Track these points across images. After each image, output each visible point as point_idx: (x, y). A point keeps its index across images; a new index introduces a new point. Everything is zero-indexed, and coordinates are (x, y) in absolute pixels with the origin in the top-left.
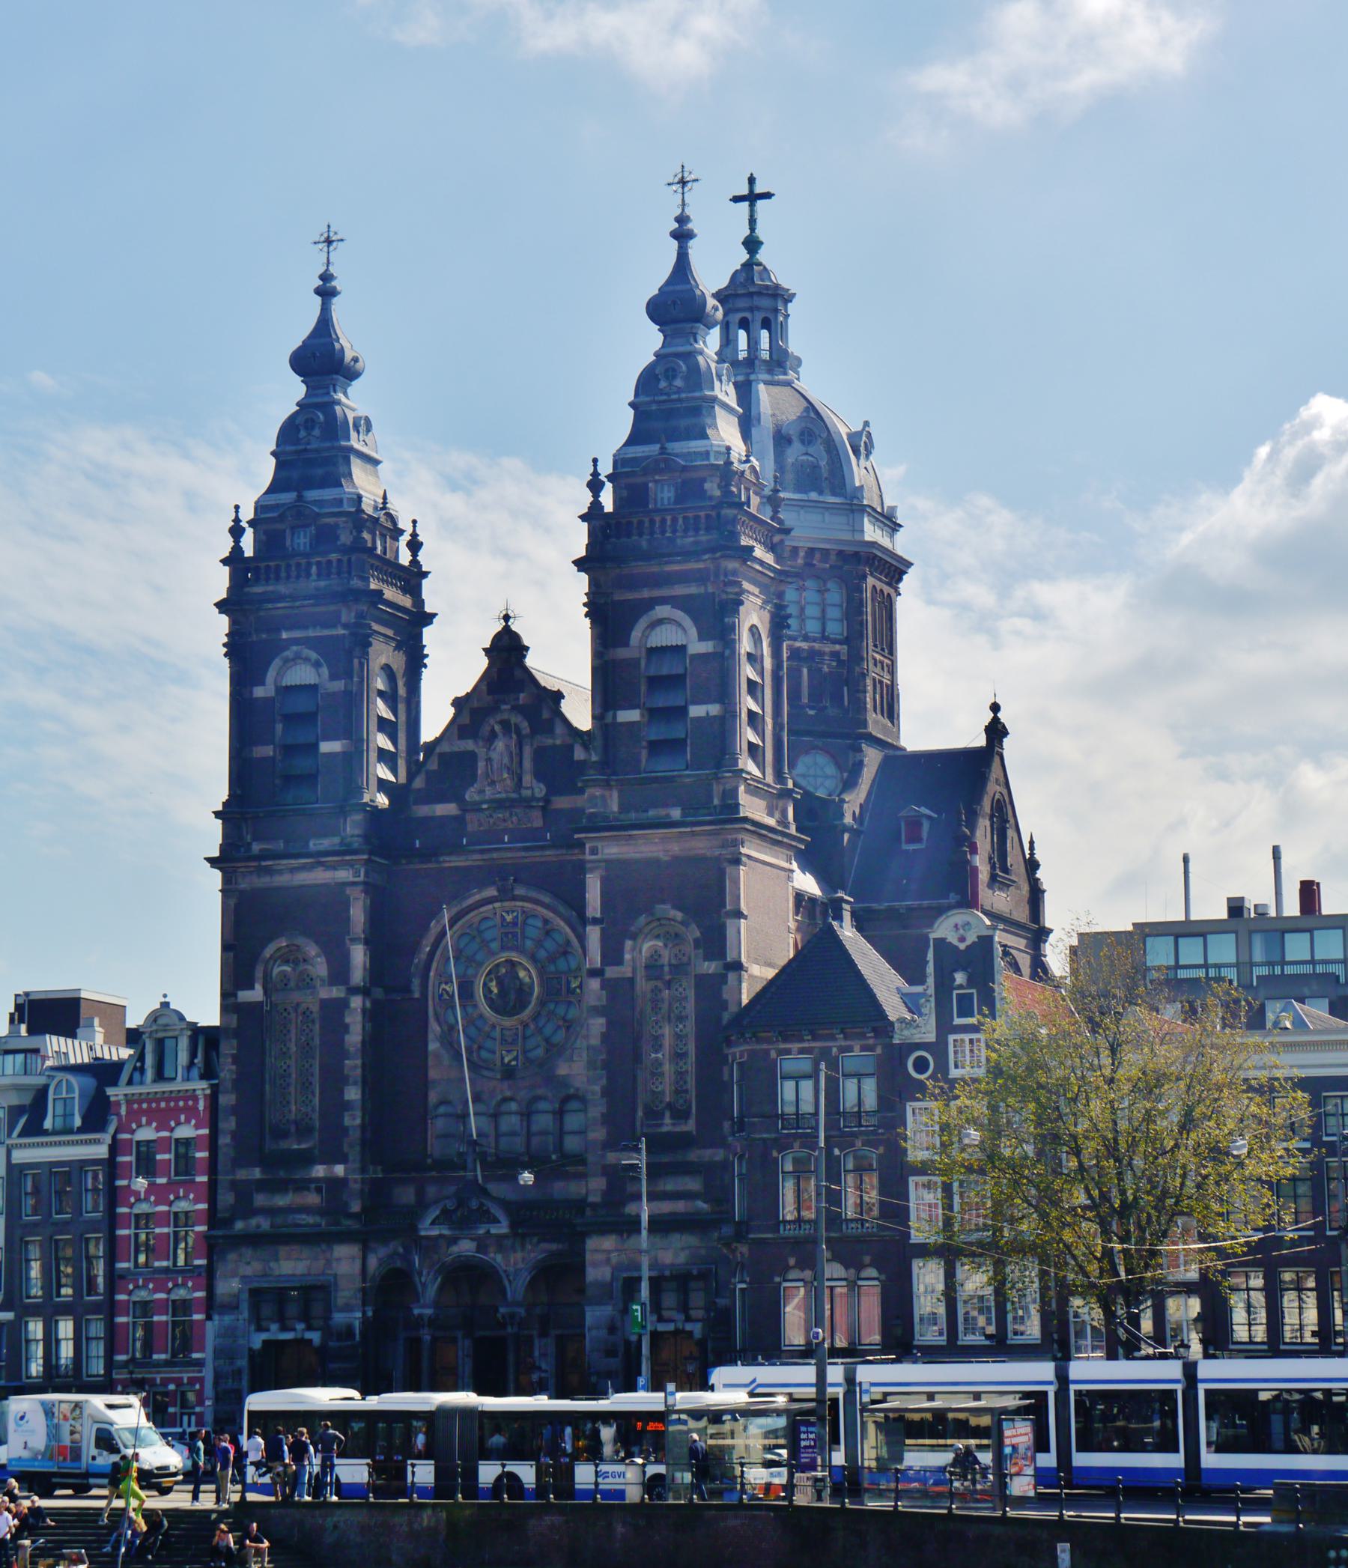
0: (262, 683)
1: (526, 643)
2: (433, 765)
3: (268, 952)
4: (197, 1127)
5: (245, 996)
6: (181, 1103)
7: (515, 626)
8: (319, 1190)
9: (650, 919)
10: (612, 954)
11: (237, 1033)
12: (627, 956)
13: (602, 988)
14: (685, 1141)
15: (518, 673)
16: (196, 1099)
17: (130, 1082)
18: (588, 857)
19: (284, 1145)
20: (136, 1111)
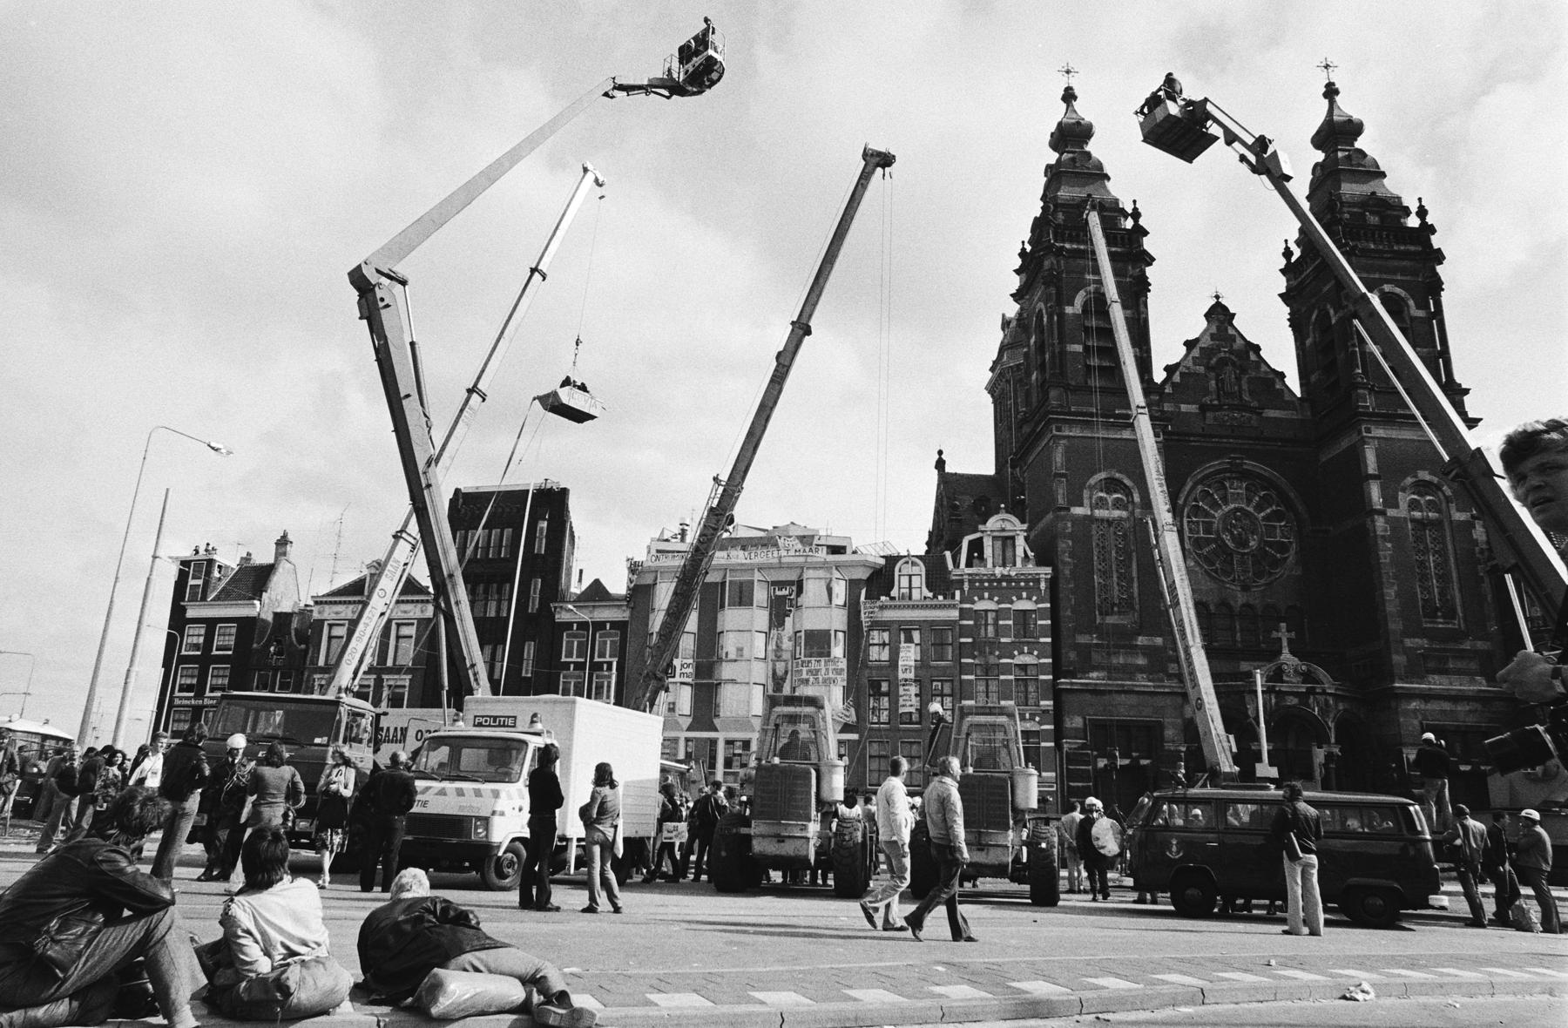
0: (1073, 305)
1: (1232, 311)
2: (1177, 378)
3: (1092, 481)
4: (1036, 602)
5: (1078, 511)
6: (1022, 584)
7: (1223, 301)
8: (1144, 654)
9: (1414, 480)
10: (1391, 501)
11: (1071, 536)
12: (1401, 503)
13: (1386, 523)
14: (1457, 636)
15: (1231, 331)
16: (1038, 581)
17: (969, 564)
18: (1365, 434)
19: (1110, 620)
20: (978, 588)
